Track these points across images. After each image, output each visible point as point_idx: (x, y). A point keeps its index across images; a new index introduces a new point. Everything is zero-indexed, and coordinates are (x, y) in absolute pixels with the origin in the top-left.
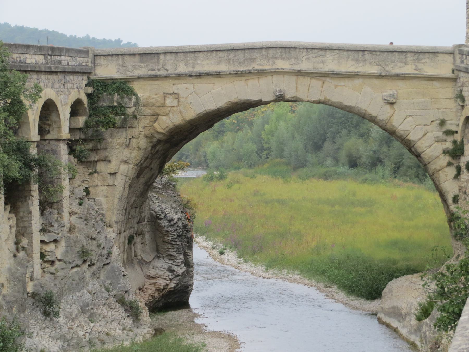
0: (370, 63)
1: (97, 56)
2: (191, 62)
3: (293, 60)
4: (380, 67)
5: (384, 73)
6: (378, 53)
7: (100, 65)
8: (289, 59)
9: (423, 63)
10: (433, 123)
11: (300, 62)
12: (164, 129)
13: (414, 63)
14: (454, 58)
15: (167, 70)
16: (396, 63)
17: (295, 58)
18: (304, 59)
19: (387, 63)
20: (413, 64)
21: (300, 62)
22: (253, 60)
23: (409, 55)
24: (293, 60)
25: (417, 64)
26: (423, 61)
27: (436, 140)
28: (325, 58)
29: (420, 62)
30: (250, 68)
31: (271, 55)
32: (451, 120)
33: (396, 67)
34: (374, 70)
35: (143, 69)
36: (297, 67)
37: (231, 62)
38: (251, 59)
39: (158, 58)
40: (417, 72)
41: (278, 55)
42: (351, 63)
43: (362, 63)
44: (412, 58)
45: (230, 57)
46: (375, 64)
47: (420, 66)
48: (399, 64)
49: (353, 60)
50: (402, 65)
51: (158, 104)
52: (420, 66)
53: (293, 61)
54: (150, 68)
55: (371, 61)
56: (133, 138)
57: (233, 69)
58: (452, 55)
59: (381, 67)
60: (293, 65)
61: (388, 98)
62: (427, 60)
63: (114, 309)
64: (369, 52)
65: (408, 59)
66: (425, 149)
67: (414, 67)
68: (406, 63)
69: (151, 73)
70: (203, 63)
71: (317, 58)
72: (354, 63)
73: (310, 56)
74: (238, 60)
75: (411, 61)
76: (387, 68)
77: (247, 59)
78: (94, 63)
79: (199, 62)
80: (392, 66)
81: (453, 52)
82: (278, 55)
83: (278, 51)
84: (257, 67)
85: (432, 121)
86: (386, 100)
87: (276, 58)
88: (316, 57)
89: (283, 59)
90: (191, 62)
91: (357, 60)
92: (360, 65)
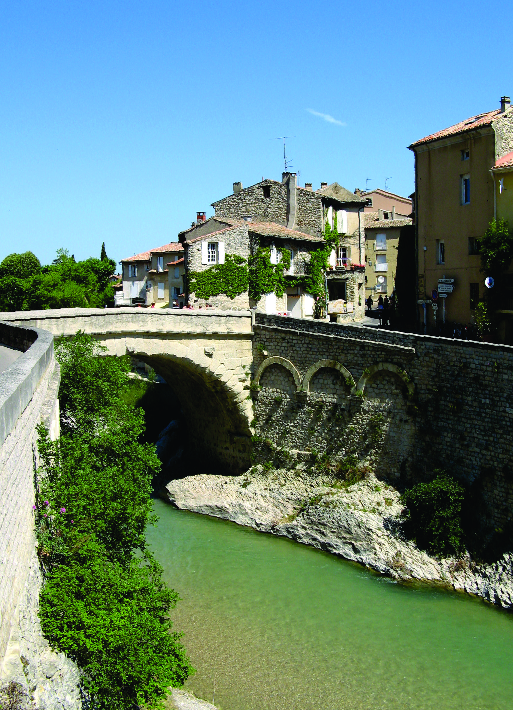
2: (62, 325)
6: (202, 317)
8: (138, 321)
14: (251, 320)
18: (149, 322)
22: (111, 323)
23: (223, 318)
24: (141, 322)
26: (231, 322)
31: (125, 319)
34: (199, 330)
37: (94, 325)
39: (36, 322)
40: (228, 331)
41: (130, 319)
42: (183, 324)
44: (224, 321)
45: (93, 321)
47: (230, 326)
49: (184, 322)
50: (217, 325)
52: (230, 326)
53: (141, 323)
61: (210, 352)
62: (234, 322)
65: (222, 321)
70: (71, 326)
72: (184, 324)
74: (99, 323)
79: (68, 325)
82: (130, 319)
83: (131, 315)
86: (207, 352)
87: (129, 322)
89: (134, 322)
90: (62, 325)
91: (187, 322)
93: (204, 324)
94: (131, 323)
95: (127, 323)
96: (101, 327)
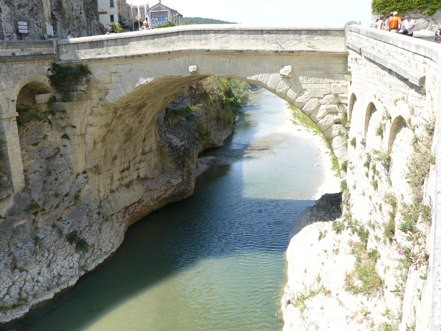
0: (268, 42)
1: (60, 45)
3: (203, 41)
4: (276, 44)
5: (280, 49)
7: (63, 53)
9: (316, 40)
10: (326, 97)
11: (209, 43)
12: (113, 101)
13: (307, 40)
15: (110, 54)
16: (291, 40)
17: (205, 39)
18: (212, 40)
19: (283, 41)
20: (306, 41)
21: (209, 43)
24: (203, 41)
25: (310, 41)
27: (329, 112)
28: (230, 38)
29: (313, 39)
30: (170, 50)
32: (343, 93)
33: (291, 45)
34: (273, 47)
35: (92, 54)
36: (206, 48)
37: (156, 45)
38: (171, 42)
40: (310, 49)
43: (261, 42)
46: (273, 42)
47: (313, 43)
48: (295, 42)
50: (297, 42)
51: (105, 81)
52: (313, 43)
54: (97, 52)
55: (269, 39)
56: (94, 107)
57: (157, 51)
58: (343, 33)
59: (278, 45)
60: (203, 45)
63: (62, 248)
64: (267, 31)
66: (318, 120)
67: (307, 44)
68: (300, 41)
69: (98, 57)
70: (136, 47)
71: (223, 38)
72: (254, 41)
73: (217, 37)
75: (305, 39)
76: (283, 46)
77: (168, 42)
78: (58, 50)
80: (287, 44)
81: (343, 29)
84: (176, 49)
85: (325, 95)
88: (222, 38)
89: (195, 40)
92: (259, 44)
93: (279, 41)
94: (193, 42)
95: (189, 41)
96: (163, 46)
